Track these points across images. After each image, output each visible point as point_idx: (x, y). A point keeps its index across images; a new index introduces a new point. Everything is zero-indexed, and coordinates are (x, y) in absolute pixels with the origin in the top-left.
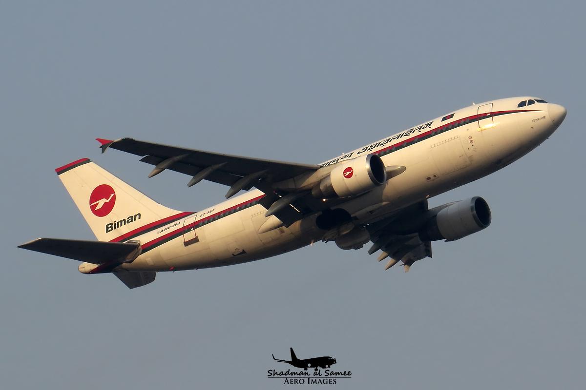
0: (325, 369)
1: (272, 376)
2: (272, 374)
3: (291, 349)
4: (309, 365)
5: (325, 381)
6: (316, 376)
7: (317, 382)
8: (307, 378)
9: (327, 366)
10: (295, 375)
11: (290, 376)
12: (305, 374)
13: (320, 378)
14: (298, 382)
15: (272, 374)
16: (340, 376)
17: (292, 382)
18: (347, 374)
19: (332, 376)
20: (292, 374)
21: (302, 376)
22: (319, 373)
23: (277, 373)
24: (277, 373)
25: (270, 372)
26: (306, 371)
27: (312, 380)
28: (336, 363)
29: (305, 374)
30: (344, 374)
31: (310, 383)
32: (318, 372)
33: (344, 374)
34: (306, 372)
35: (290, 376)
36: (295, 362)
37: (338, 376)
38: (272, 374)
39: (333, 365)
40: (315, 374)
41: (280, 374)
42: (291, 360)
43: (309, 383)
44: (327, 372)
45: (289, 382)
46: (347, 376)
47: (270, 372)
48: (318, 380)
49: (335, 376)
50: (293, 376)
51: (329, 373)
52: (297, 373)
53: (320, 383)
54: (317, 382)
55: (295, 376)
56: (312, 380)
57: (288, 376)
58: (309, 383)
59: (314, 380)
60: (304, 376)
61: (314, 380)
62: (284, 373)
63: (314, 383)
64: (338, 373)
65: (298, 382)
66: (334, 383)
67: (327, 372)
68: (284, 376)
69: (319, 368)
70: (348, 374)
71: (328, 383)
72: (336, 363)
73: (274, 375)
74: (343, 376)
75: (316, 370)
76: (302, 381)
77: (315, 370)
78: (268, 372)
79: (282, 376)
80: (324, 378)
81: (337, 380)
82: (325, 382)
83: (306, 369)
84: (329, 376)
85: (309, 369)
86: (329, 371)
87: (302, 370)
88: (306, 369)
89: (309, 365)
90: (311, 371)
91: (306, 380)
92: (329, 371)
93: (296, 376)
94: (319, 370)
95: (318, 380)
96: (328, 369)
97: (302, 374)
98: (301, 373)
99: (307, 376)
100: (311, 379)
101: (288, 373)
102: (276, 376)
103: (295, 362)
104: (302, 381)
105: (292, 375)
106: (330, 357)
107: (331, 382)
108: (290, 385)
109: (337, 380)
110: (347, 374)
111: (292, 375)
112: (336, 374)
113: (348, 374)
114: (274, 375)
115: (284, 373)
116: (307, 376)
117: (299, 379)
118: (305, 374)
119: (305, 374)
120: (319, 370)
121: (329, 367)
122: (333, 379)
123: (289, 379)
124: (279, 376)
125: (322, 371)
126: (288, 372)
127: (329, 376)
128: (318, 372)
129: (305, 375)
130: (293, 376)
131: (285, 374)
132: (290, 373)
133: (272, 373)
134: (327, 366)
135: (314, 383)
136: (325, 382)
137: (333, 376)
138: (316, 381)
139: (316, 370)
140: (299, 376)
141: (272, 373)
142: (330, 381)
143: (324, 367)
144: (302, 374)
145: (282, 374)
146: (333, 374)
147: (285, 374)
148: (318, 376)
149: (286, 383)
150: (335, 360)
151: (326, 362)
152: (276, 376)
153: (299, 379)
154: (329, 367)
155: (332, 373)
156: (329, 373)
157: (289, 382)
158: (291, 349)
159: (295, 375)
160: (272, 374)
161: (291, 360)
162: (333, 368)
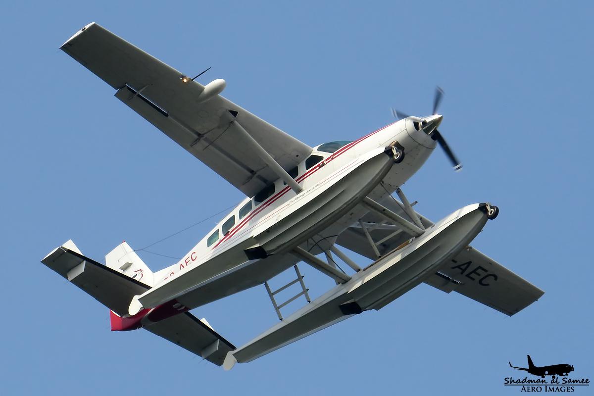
0: (563, 377)
1: (509, 384)
3: (528, 356)
4: (547, 373)
5: (563, 389)
6: (553, 384)
7: (555, 390)
8: (545, 386)
9: (564, 374)
10: (532, 382)
11: (528, 384)
12: (543, 381)
13: (558, 386)
14: (535, 390)
15: (509, 382)
16: (578, 383)
17: (529, 390)
19: (569, 384)
21: (539, 384)
22: (556, 381)
23: (513, 381)
24: (513, 381)
25: (507, 379)
26: (543, 379)
27: (550, 388)
28: (573, 370)
29: (543, 382)
30: (582, 382)
31: (548, 391)
32: (555, 380)
33: (582, 382)
34: (544, 379)
35: (528, 384)
36: (533, 369)
37: (575, 383)
39: (571, 372)
40: (553, 382)
41: (517, 382)
42: (528, 368)
43: (546, 391)
44: (564, 379)
45: (526, 390)
46: (585, 384)
47: (507, 379)
48: (555, 387)
50: (531, 383)
51: (567, 380)
52: (534, 381)
53: (557, 391)
54: (555, 390)
55: (532, 384)
56: (550, 388)
57: (525, 383)
58: (546, 391)
59: (551, 388)
60: (541, 383)
61: (551, 388)
63: (551, 391)
64: (576, 380)
65: (535, 390)
66: (572, 391)
67: (564, 379)
68: (521, 384)
69: (556, 376)
70: (586, 382)
71: (566, 390)
72: (573, 370)
73: (511, 382)
74: (581, 384)
75: (554, 377)
78: (505, 379)
79: (519, 384)
81: (575, 388)
82: (563, 390)
83: (543, 377)
85: (546, 376)
87: (540, 377)
88: (543, 377)
89: (547, 373)
90: (548, 378)
91: (544, 388)
93: (533, 383)
94: (556, 378)
95: (555, 387)
96: (566, 376)
97: (539, 381)
98: (539, 381)
99: (544, 383)
100: (548, 387)
101: (525, 381)
102: (513, 383)
103: (533, 369)
105: (529, 383)
106: (567, 365)
107: (569, 390)
108: (527, 393)
109: (575, 388)
111: (529, 383)
112: (574, 382)
113: (586, 382)
114: (511, 382)
116: (544, 383)
117: (536, 387)
118: (543, 382)
119: (543, 381)
120: (556, 378)
121: (567, 375)
122: (571, 386)
123: (526, 387)
124: (516, 384)
125: (560, 379)
126: (525, 380)
127: (567, 384)
128: (555, 380)
129: (542, 383)
130: (531, 383)
131: (522, 382)
133: (509, 380)
134: (564, 374)
135: (551, 391)
136: (563, 390)
137: (570, 383)
138: (553, 388)
139: (554, 377)
140: (536, 384)
141: (509, 380)
143: (561, 375)
144: (539, 381)
146: (570, 381)
147: (522, 382)
148: (556, 384)
149: (524, 391)
151: (563, 369)
152: (513, 383)
154: (567, 375)
155: (570, 381)
156: (567, 380)
157: (526, 390)
158: (528, 356)
159: (532, 382)
160: (509, 382)
161: (528, 368)
162: (571, 376)
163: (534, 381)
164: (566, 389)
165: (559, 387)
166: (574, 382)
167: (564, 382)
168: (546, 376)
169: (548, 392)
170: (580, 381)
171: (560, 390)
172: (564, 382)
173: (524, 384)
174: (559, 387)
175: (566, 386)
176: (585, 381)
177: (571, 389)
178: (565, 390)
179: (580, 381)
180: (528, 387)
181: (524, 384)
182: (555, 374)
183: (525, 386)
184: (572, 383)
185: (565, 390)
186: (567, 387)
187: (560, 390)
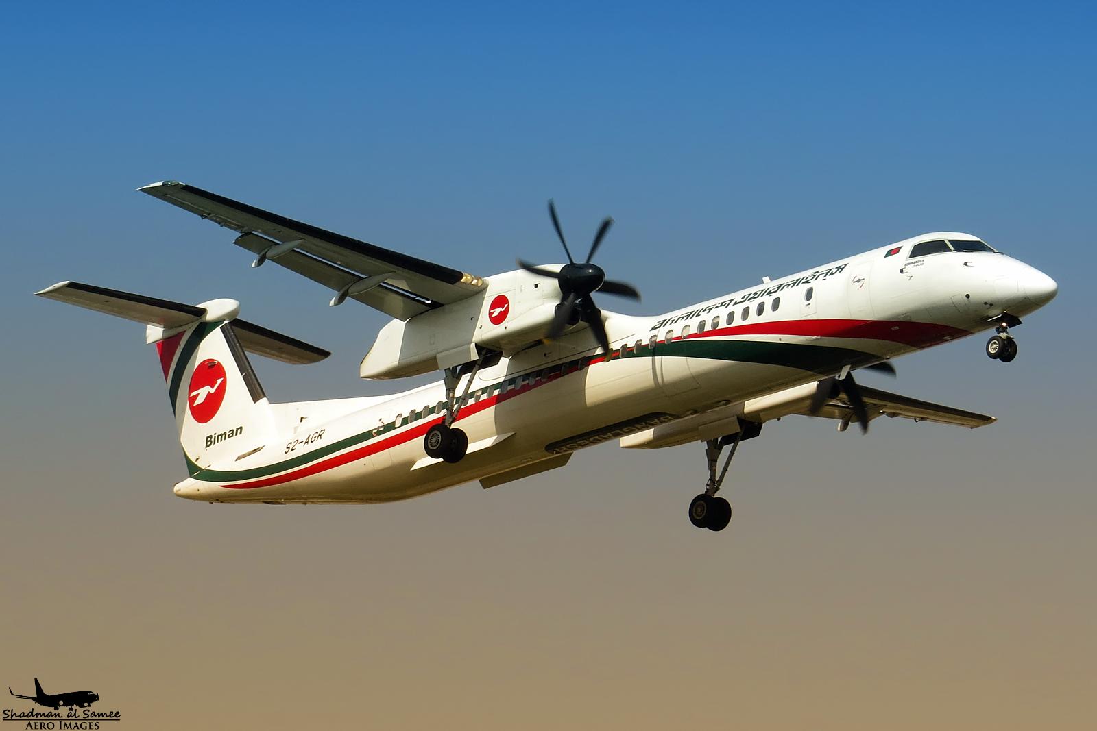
1: (9, 718)
3: (36, 680)
4: (61, 703)
5: (83, 726)
6: (70, 718)
7: (73, 727)
8: (59, 722)
9: (86, 704)
10: (41, 716)
11: (35, 718)
12: (56, 715)
13: (75, 721)
14: (46, 726)
15: (9, 715)
16: (105, 718)
17: (37, 727)
18: (115, 716)
20: (37, 715)
21: (51, 718)
22: (75, 714)
23: (15, 714)
24: (15, 714)
25: (6, 712)
27: (65, 724)
28: (98, 699)
29: (56, 715)
30: (110, 716)
32: (73, 713)
33: (110, 716)
34: (57, 712)
35: (35, 718)
36: (42, 698)
37: (101, 718)
39: (95, 702)
40: (69, 715)
41: (20, 716)
42: (36, 696)
44: (86, 712)
45: (33, 726)
46: (115, 718)
47: (6, 712)
48: (73, 723)
50: (39, 718)
51: (90, 713)
52: (44, 714)
54: (73, 727)
56: (65, 724)
57: (31, 718)
59: (68, 725)
60: (53, 718)
62: (25, 714)
63: (67, 728)
64: (102, 714)
65: (46, 726)
66: (96, 727)
67: (86, 712)
68: (26, 718)
69: (75, 707)
70: (116, 716)
71: (88, 727)
73: (12, 717)
74: (109, 718)
75: (71, 709)
78: (4, 712)
79: (23, 718)
81: (101, 724)
82: (84, 727)
83: (56, 709)
84: (89, 718)
85: (60, 708)
86: (88, 711)
87: (52, 709)
88: (56, 709)
89: (61, 703)
90: (64, 711)
92: (88, 711)
93: (43, 718)
94: (74, 710)
95: (73, 723)
96: (88, 708)
98: (50, 714)
99: (57, 718)
102: (14, 717)
103: (42, 698)
105: (37, 717)
107: (92, 727)
109: (101, 724)
110: (115, 716)
111: (37, 717)
112: (99, 715)
113: (116, 716)
114: (12, 716)
115: (25, 714)
116: (57, 718)
117: (46, 722)
118: (56, 715)
119: (56, 715)
120: (74, 710)
121: (89, 706)
122: (95, 722)
123: (33, 723)
124: (19, 718)
125: (80, 711)
126: (32, 713)
127: (89, 718)
128: (73, 713)
130: (39, 718)
131: (27, 716)
132: (34, 714)
133: (10, 713)
134: (86, 704)
135: (67, 728)
136: (84, 727)
137: (94, 718)
138: (70, 724)
139: (71, 709)
140: (46, 718)
141: (10, 713)
142: (90, 725)
143: (82, 706)
144: (51, 715)
145: (23, 716)
146: (94, 715)
147: (27, 716)
148: (74, 718)
149: (29, 728)
150: (97, 696)
151: (84, 698)
152: (14, 717)
153: (46, 722)
154: (89, 706)
155: (94, 714)
156: (90, 713)
157: (33, 726)
158: (36, 680)
159: (41, 716)
160: (9, 715)
161: (36, 696)
162: (95, 707)
164: (88, 725)
166: (99, 715)
170: (108, 715)
173: (30, 718)
174: (79, 723)
176: (114, 714)
177: (94, 726)
178: (86, 727)
179: (108, 715)
180: (35, 723)
181: (30, 718)
182: (73, 705)
184: (97, 718)
185: (86, 727)
186: (90, 723)
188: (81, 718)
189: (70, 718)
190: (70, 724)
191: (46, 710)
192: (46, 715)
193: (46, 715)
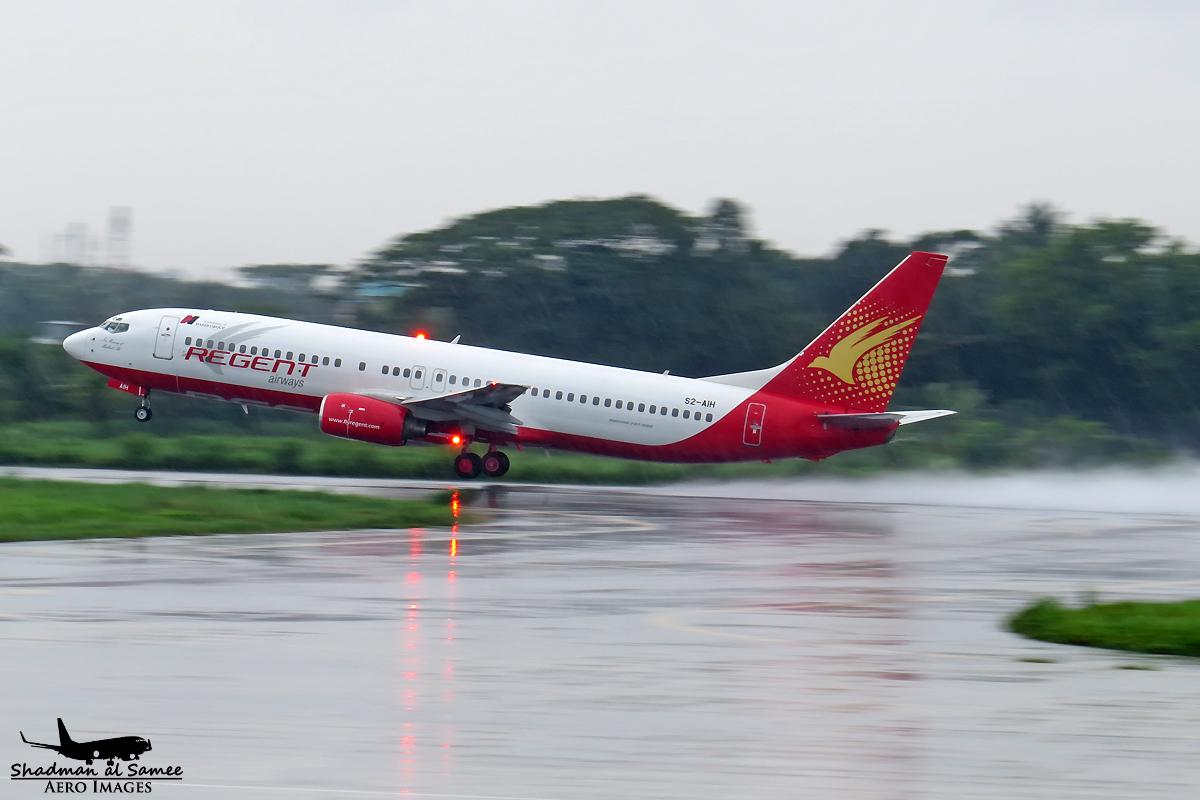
0: (129, 763)
1: (21, 776)
2: (19, 772)
3: (60, 720)
4: (96, 754)
5: (129, 787)
6: (110, 776)
8: (92, 782)
9: (132, 756)
10: (67, 774)
11: (58, 776)
12: (88, 772)
13: (118, 781)
14: (73, 788)
15: (20, 772)
16: (160, 775)
17: (61, 789)
18: (174, 773)
21: (81, 776)
22: (116, 771)
23: (29, 770)
24: (29, 770)
25: (16, 768)
26: (89, 766)
27: (102, 785)
28: (150, 749)
30: (168, 773)
31: (98, 790)
32: (114, 768)
33: (168, 773)
34: (91, 767)
35: (58, 776)
36: (68, 747)
37: (154, 775)
38: (19, 772)
39: (145, 753)
40: (108, 772)
41: (35, 773)
42: (59, 744)
43: (95, 791)
45: (56, 789)
46: (174, 776)
47: (16, 768)
48: (114, 784)
49: (148, 776)
50: (64, 775)
51: (138, 769)
52: (71, 770)
53: (118, 791)
54: (113, 789)
56: (102, 785)
57: (53, 776)
58: (95, 791)
60: (85, 776)
61: (106, 783)
62: (44, 771)
63: (105, 790)
64: (156, 769)
65: (73, 788)
66: (148, 790)
67: (132, 768)
68: (45, 776)
69: (116, 760)
70: (176, 773)
71: (136, 790)
72: (150, 749)
73: (24, 774)
74: (166, 776)
75: (110, 763)
76: (81, 788)
77: (109, 763)
78: (13, 767)
79: (41, 776)
80: (126, 781)
81: (154, 784)
83: (89, 762)
84: (137, 776)
85: (95, 761)
87: (82, 763)
88: (89, 762)
89: (96, 754)
90: (99, 765)
91: (90, 784)
93: (70, 775)
94: (115, 764)
95: (114, 784)
96: (135, 761)
97: (82, 772)
98: (80, 770)
99: (91, 776)
100: (99, 782)
101: (54, 770)
102: (28, 775)
103: (68, 747)
104: (81, 788)
105: (61, 774)
106: (138, 738)
107: (141, 789)
109: (154, 784)
110: (174, 773)
111: (61, 774)
112: (152, 772)
113: (176, 773)
114: (24, 774)
115: (44, 771)
116: (91, 776)
117: (74, 782)
119: (88, 772)
120: (115, 764)
121: (137, 758)
122: (145, 782)
123: (54, 783)
124: (34, 776)
125: (123, 766)
126: (53, 768)
127: (137, 776)
128: (114, 768)
130: (64, 775)
133: (21, 769)
135: (105, 790)
137: (144, 776)
138: (109, 786)
139: (110, 763)
140: (75, 776)
141: (21, 769)
142: (138, 787)
143: (126, 758)
144: (82, 772)
146: (145, 772)
147: (47, 772)
148: (115, 776)
149: (50, 790)
150: (149, 744)
151: (129, 746)
152: (28, 775)
153: (74, 782)
154: (137, 758)
155: (143, 770)
156: (138, 769)
157: (56, 789)
158: (60, 720)
159: (67, 774)
160: (20, 772)
161: (59, 744)
162: (146, 760)
163: (71, 770)
165: (122, 783)
166: (152, 772)
167: (133, 773)
168: (95, 761)
169: (98, 793)
170: (165, 771)
171: (122, 788)
172: (133, 773)
173: (49, 777)
174: (122, 783)
175: (135, 782)
176: (173, 771)
181: (49, 777)
182: (113, 757)
183: (52, 781)
187: (122, 788)
188: (125, 775)
189: (110, 776)
190: (109, 786)
191: (75, 764)
192: (73, 771)
193: (73, 771)
